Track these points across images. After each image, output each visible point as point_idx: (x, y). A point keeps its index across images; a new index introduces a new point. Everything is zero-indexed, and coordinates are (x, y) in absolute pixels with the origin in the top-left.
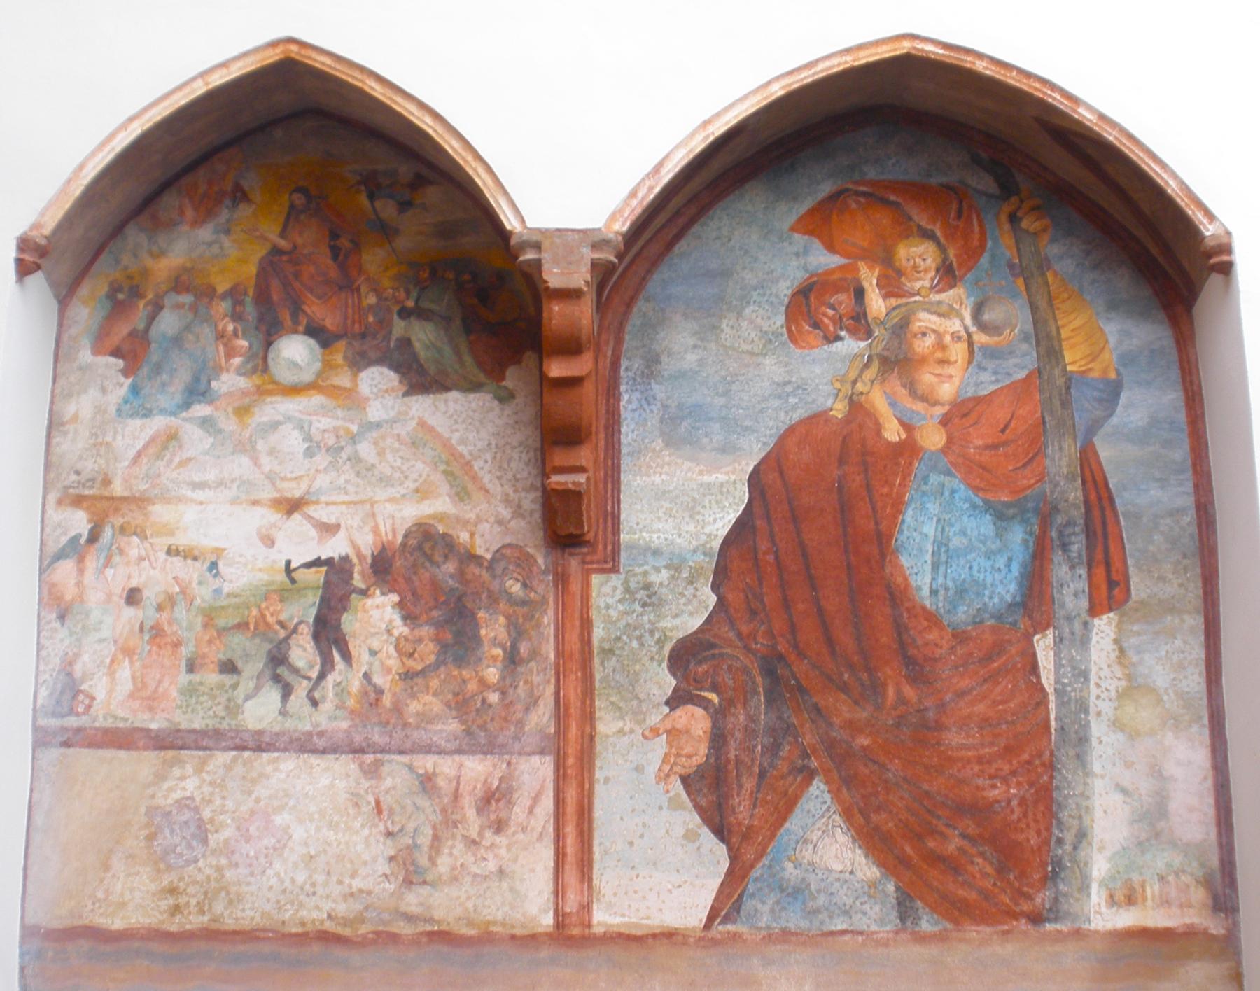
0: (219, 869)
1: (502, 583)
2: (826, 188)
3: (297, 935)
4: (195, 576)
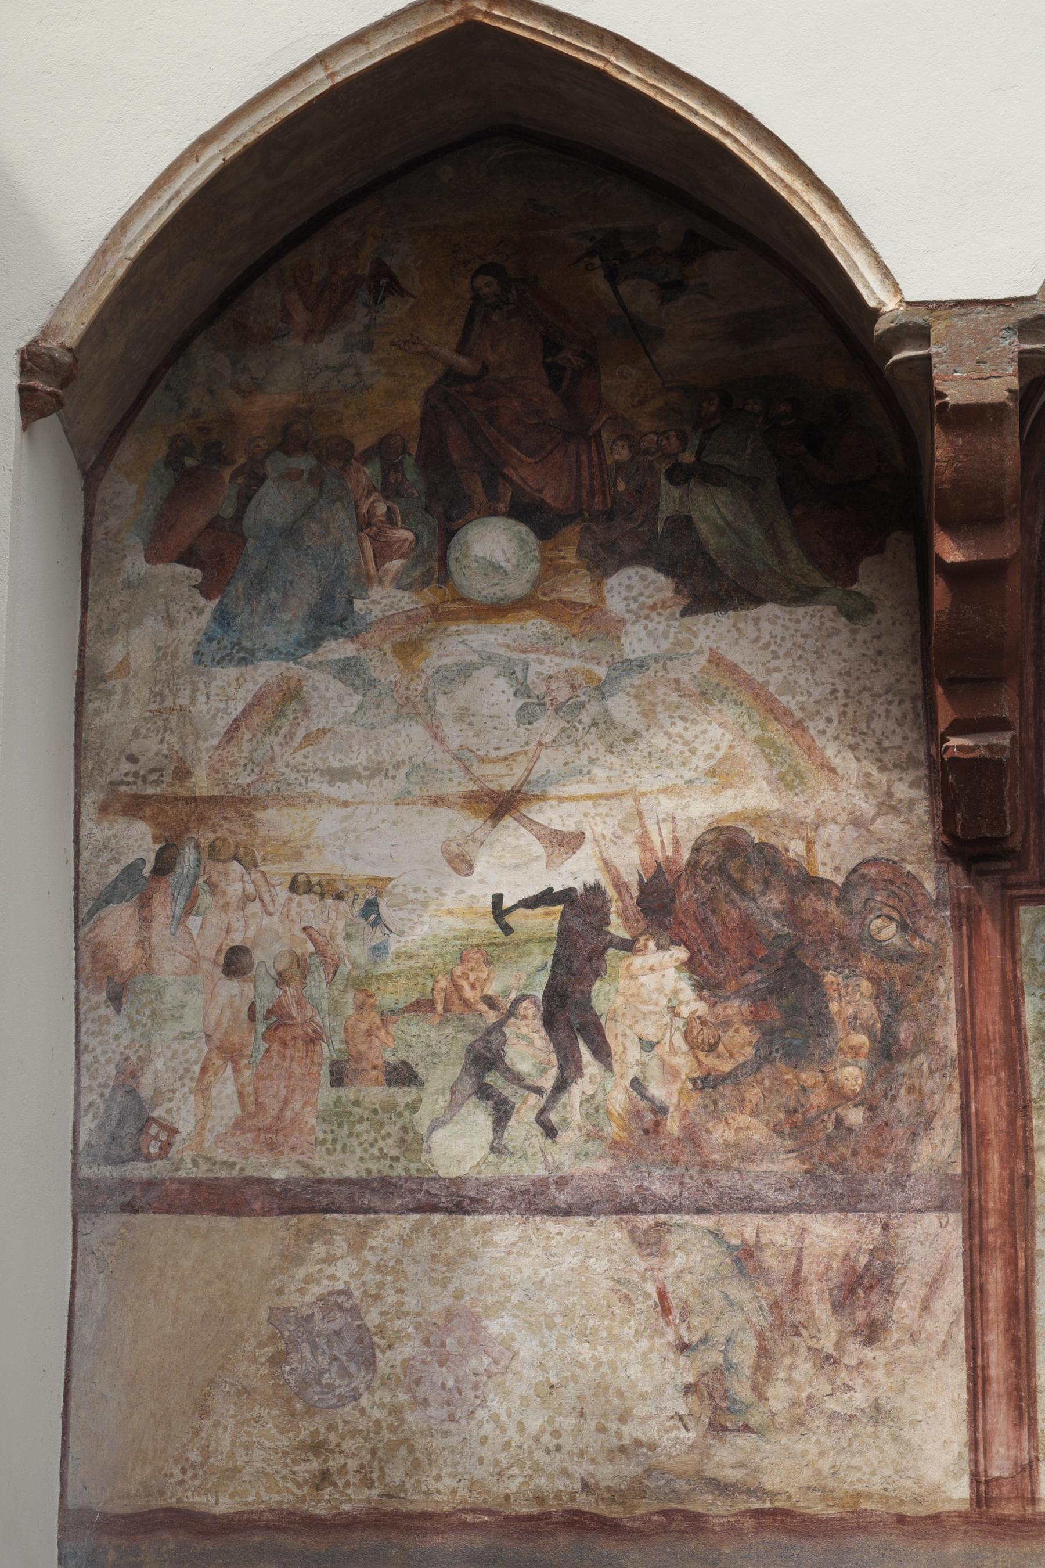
0: (396, 1411)
1: (864, 926)
3: (531, 1517)
4: (341, 924)
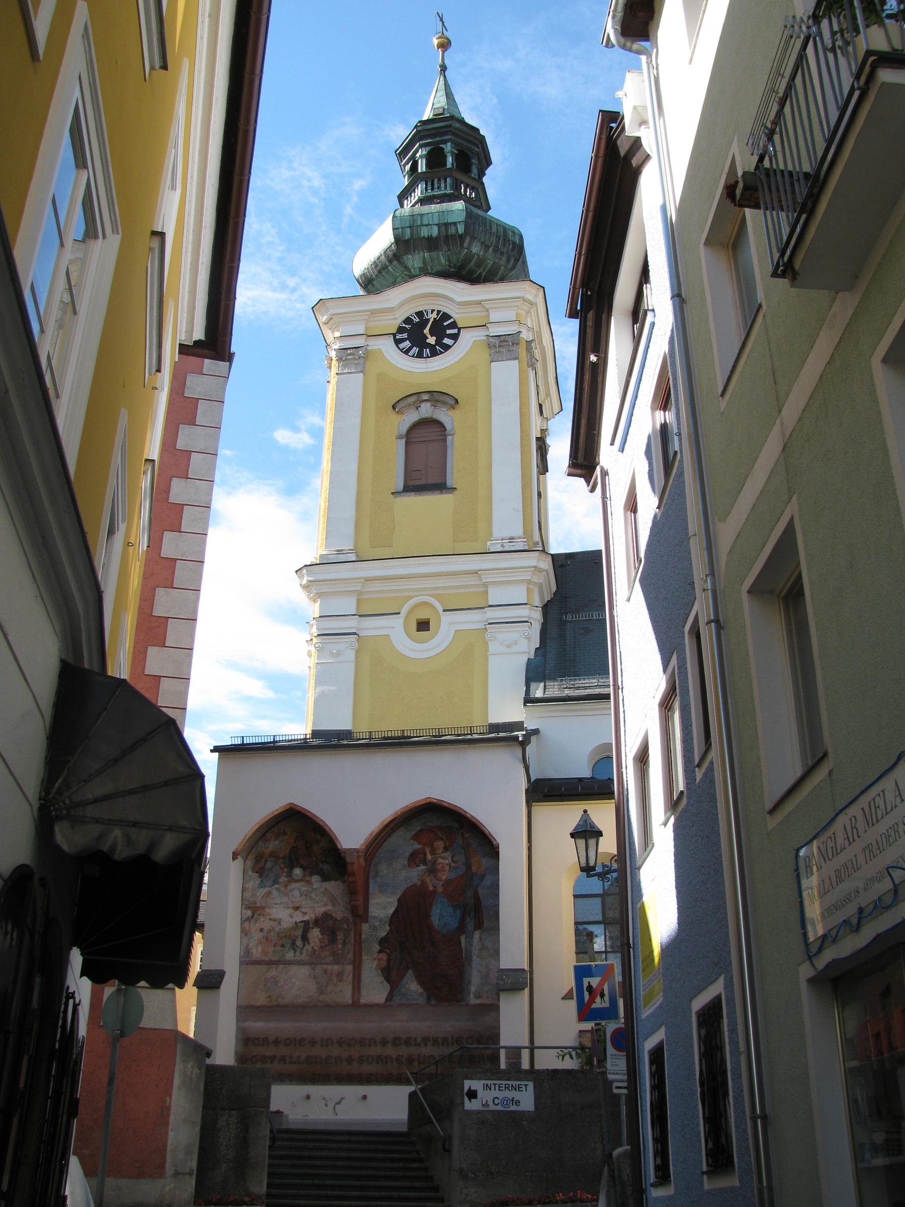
2: (419, 828)
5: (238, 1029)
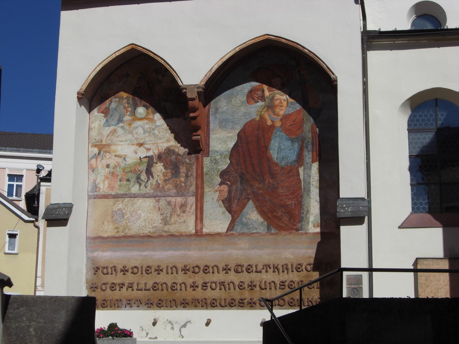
0: (126, 223)
5: (88, 258)
